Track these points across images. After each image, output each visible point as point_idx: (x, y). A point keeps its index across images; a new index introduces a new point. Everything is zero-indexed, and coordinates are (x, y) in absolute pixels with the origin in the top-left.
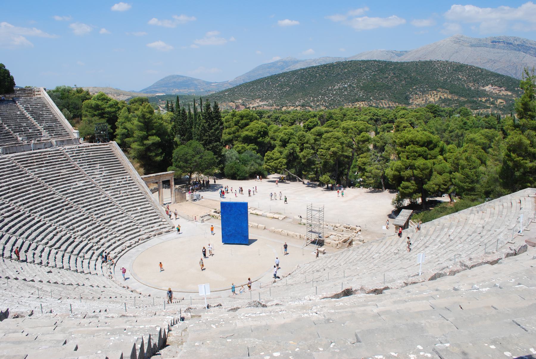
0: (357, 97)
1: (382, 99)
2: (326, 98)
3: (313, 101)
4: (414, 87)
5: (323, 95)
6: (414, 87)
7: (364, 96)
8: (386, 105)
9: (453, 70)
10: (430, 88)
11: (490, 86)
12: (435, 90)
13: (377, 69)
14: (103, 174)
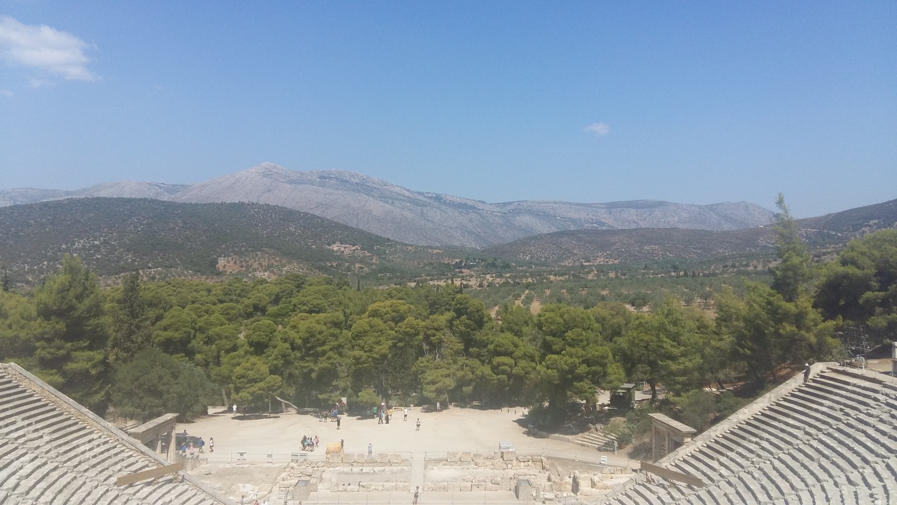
0: (122, 263)
1: (172, 267)
2: (58, 266)
3: (31, 271)
4: (224, 246)
5: (51, 261)
6: (224, 246)
7: (135, 261)
8: (180, 276)
9: (280, 219)
10: (250, 247)
11: (338, 244)
12: (259, 250)
13: (151, 214)
14: (47, 438)
